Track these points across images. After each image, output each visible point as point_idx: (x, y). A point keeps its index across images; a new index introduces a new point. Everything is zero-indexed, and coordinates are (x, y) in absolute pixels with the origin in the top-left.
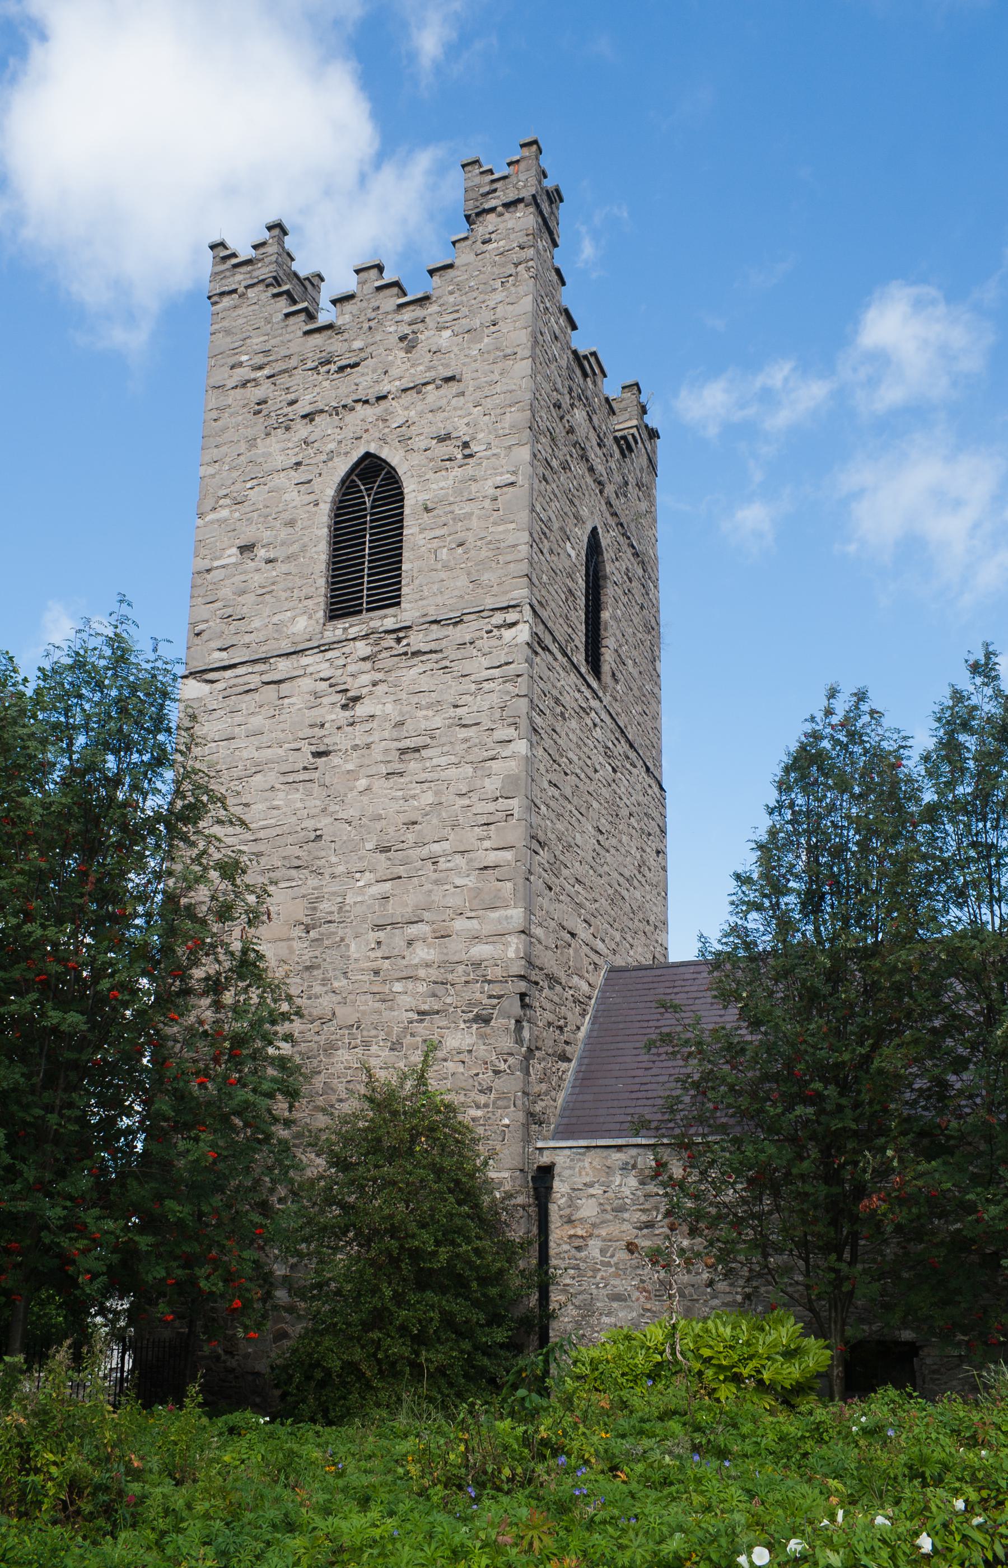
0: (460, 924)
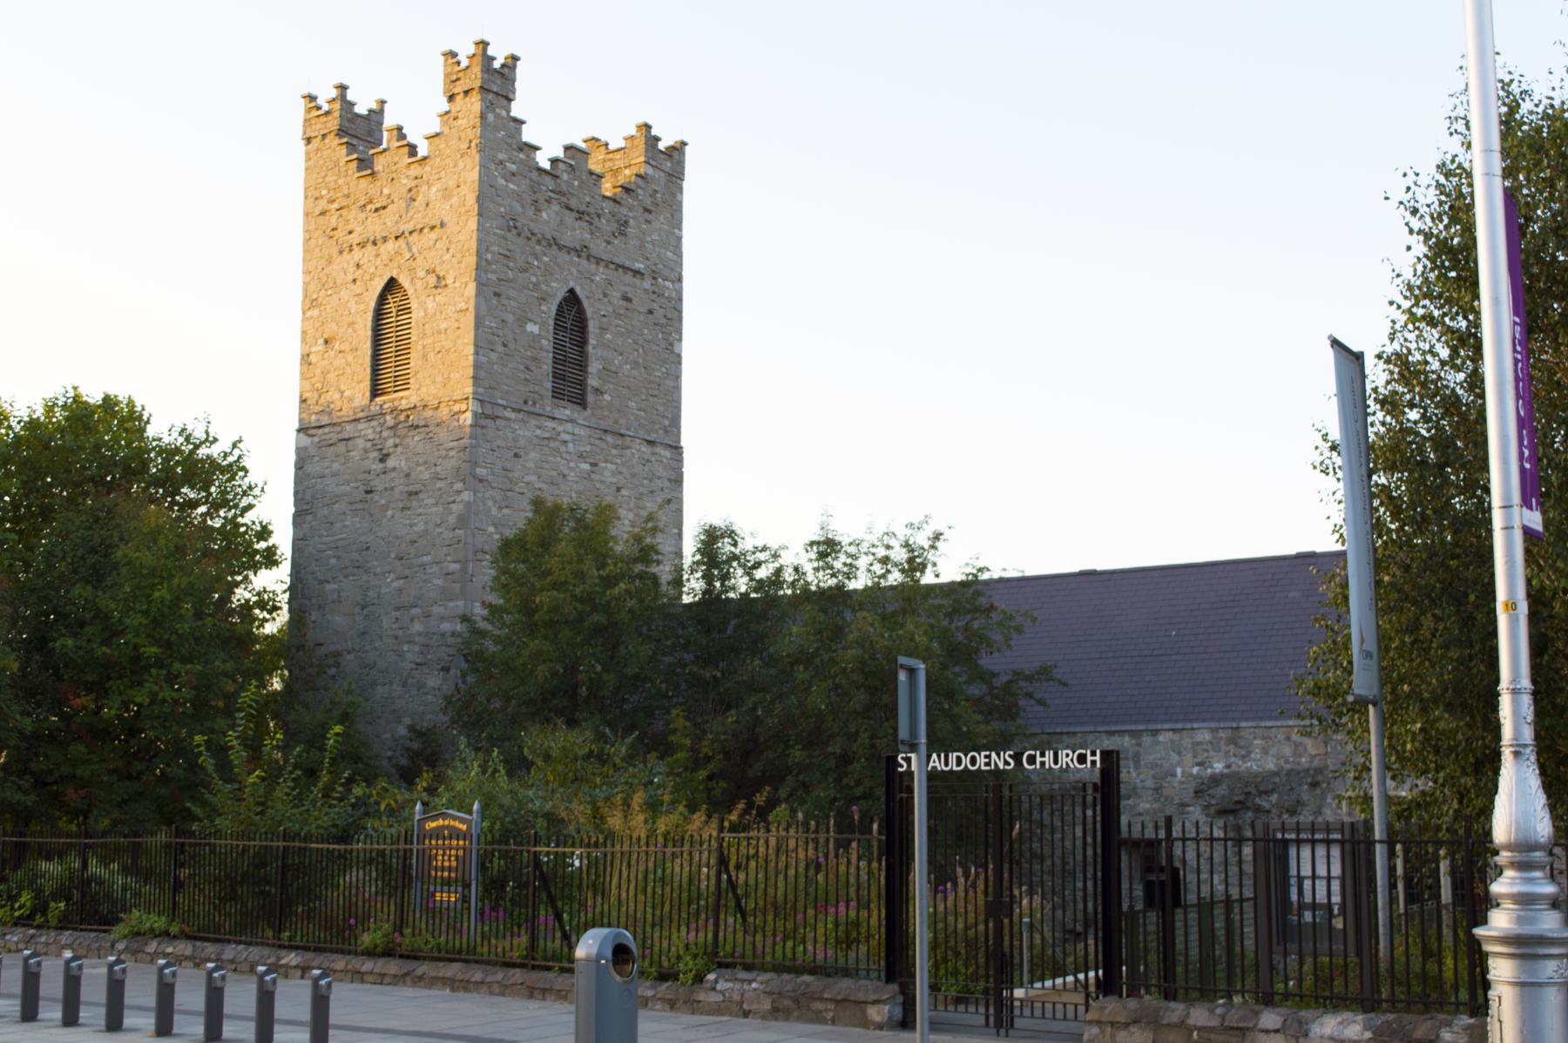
0: (436, 610)
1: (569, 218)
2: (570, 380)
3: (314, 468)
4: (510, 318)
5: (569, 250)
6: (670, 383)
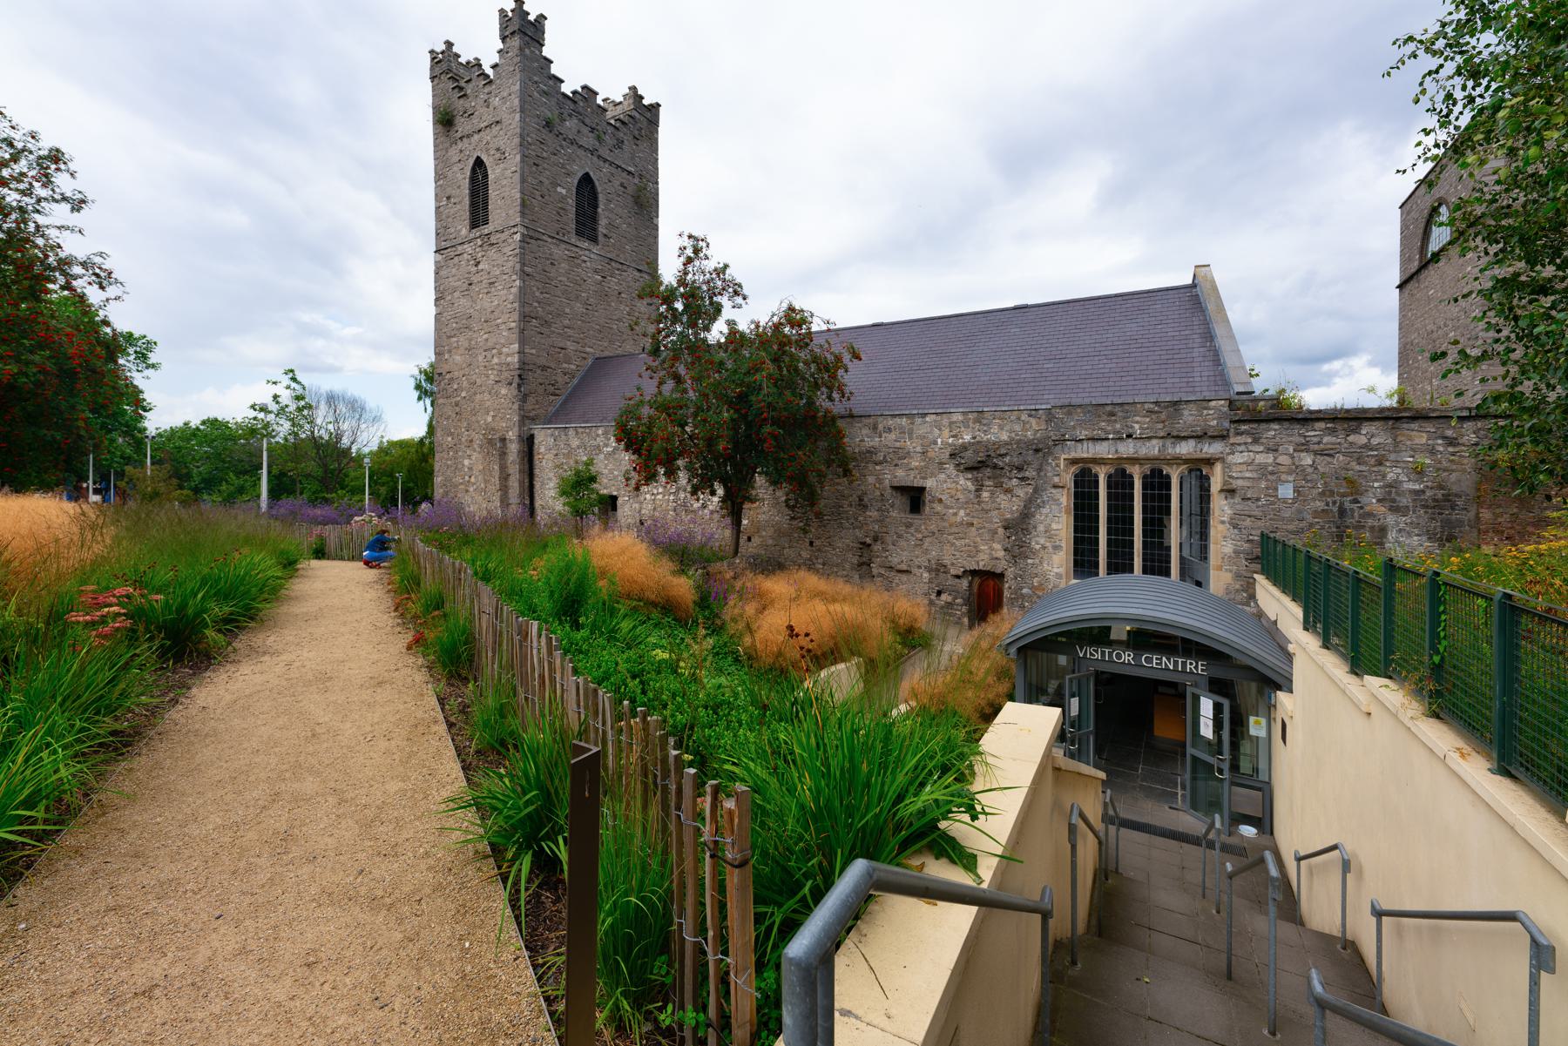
1: (585, 130)
2: (587, 224)
3: (443, 273)
4: (547, 182)
5: (586, 150)
6: (651, 240)
